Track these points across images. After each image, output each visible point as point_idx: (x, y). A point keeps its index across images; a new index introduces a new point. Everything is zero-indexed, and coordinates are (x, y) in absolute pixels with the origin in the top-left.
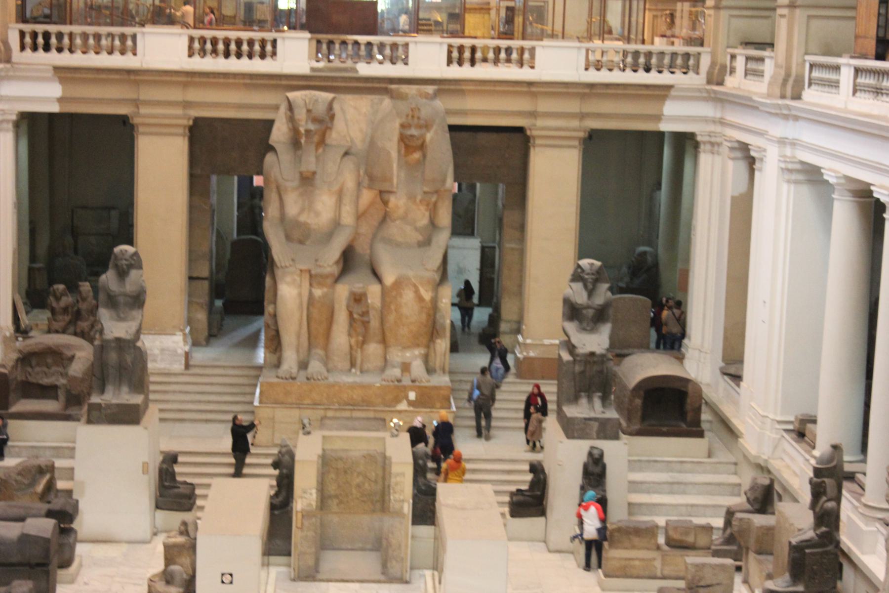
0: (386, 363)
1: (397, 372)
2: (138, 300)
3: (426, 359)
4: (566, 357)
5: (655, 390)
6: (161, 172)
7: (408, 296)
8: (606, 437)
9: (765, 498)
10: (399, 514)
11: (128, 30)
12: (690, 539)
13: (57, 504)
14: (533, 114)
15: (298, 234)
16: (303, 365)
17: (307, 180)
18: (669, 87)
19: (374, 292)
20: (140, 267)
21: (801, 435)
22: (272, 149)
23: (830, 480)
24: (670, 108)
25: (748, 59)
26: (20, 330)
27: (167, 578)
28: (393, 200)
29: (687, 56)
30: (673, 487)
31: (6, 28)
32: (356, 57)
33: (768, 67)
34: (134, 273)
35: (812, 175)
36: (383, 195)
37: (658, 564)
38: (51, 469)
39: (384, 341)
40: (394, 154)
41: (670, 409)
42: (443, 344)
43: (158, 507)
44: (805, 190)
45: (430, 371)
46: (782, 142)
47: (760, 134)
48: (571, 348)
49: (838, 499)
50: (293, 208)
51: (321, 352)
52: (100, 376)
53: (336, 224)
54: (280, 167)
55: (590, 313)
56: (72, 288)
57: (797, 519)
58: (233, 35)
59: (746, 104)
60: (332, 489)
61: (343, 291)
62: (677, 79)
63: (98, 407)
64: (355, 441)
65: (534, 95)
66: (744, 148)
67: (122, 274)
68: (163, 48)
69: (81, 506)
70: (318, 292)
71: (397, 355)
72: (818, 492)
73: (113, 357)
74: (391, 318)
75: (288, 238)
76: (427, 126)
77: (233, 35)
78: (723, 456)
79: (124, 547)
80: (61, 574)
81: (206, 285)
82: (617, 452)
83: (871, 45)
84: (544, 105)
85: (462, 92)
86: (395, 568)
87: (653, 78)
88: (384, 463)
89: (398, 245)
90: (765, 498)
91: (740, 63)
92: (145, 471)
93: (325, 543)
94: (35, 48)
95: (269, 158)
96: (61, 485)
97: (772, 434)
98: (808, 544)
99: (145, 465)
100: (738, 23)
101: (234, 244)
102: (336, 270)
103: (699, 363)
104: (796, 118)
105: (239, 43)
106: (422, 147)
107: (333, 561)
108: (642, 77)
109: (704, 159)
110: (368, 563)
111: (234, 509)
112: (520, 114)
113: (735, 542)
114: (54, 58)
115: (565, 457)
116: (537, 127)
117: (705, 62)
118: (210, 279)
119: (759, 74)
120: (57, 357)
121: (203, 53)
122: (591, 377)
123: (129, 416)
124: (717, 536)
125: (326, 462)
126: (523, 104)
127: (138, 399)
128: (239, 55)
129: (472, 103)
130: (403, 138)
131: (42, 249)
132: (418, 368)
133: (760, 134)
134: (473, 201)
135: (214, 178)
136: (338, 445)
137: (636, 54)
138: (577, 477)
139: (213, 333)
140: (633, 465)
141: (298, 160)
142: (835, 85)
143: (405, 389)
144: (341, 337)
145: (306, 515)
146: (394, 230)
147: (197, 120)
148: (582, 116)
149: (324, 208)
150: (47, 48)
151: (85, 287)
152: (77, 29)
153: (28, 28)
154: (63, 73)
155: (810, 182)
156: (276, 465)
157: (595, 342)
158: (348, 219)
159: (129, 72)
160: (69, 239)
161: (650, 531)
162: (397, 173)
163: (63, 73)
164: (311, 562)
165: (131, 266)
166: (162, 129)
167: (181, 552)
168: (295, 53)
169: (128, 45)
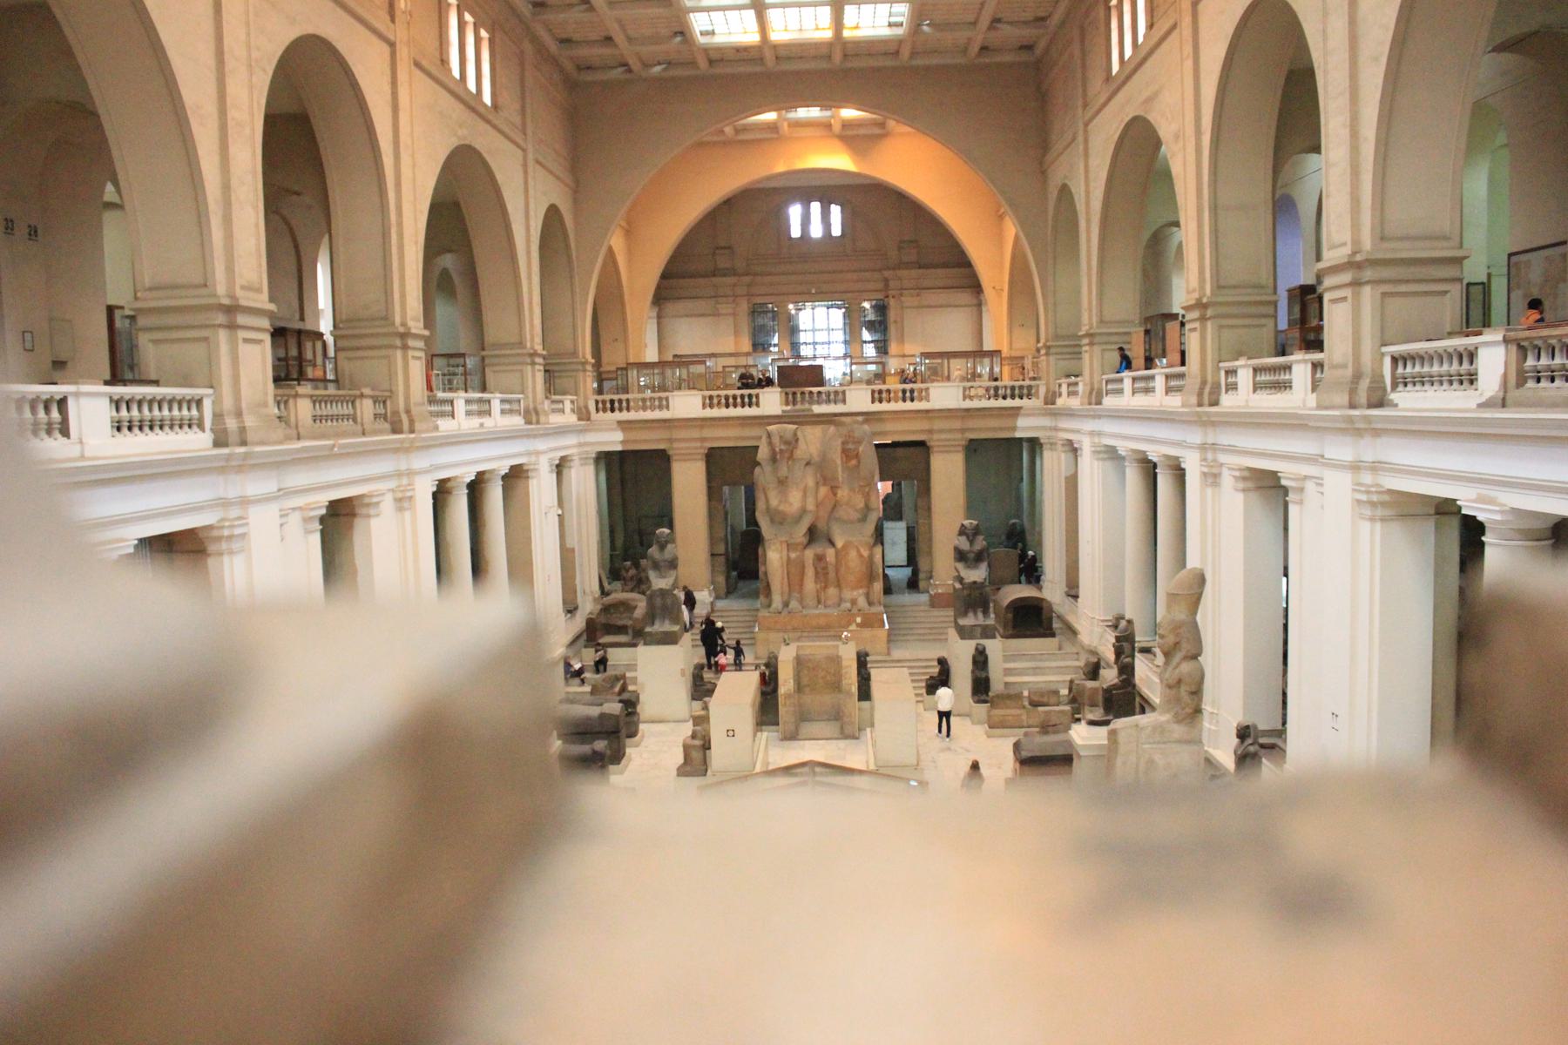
0: (841, 600)
1: (848, 605)
2: (673, 564)
3: (867, 595)
4: (958, 586)
5: (1023, 607)
6: (688, 483)
7: (853, 554)
8: (987, 637)
9: (1094, 671)
10: (849, 693)
11: (663, 395)
12: (1045, 700)
13: (625, 696)
14: (930, 432)
15: (778, 519)
16: (786, 605)
17: (782, 483)
18: (1019, 408)
19: (830, 553)
20: (673, 541)
21: (1116, 627)
22: (759, 464)
23: (1125, 644)
24: (1022, 422)
25: (1069, 385)
26: (604, 593)
27: (694, 736)
28: (840, 493)
29: (1030, 388)
30: (1036, 671)
31: (586, 398)
32: (811, 403)
33: (1080, 388)
34: (669, 546)
35: (1112, 454)
36: (834, 490)
37: (1024, 717)
38: (624, 677)
39: (839, 586)
40: (839, 462)
41: (1031, 620)
42: (878, 586)
43: (694, 699)
44: (1108, 464)
45: (870, 604)
46: (1092, 433)
47: (1078, 431)
48: (960, 579)
49: (1133, 657)
50: (774, 502)
51: (796, 595)
52: (651, 617)
53: (804, 511)
54: (764, 476)
55: (972, 556)
56: (637, 565)
57: (1110, 676)
58: (730, 393)
59: (1070, 413)
60: (805, 681)
61: (809, 554)
62: (1025, 402)
63: (650, 634)
64: (817, 648)
65: (930, 419)
66: (1070, 442)
67: (662, 547)
68: (686, 404)
69: (642, 698)
70: (793, 555)
71: (848, 594)
72: (1119, 652)
73: (658, 602)
74: (843, 570)
75: (772, 521)
76: (859, 442)
77: (730, 393)
78: (1069, 648)
79: (672, 725)
80: (628, 741)
81: (722, 559)
82: (995, 648)
83: (1142, 361)
84: (938, 425)
85: (881, 420)
86: (848, 730)
87: (1009, 403)
88: (836, 660)
89: (845, 522)
90: (1094, 671)
91: (1064, 389)
92: (683, 674)
93: (803, 717)
94: (605, 410)
95: (757, 470)
96: (631, 688)
97: (1098, 630)
98: (1114, 687)
99: (683, 673)
100: (1062, 363)
101: (745, 534)
102: (805, 541)
103: (1052, 590)
104: (1100, 417)
105: (735, 397)
106: (857, 456)
107: (808, 728)
108: (1001, 403)
109: (1047, 454)
110: (830, 728)
111: (737, 690)
112: (922, 431)
113: (1077, 701)
114: (618, 416)
115: (960, 654)
116: (934, 441)
117: (1042, 391)
118: (726, 554)
119: (1075, 393)
120: (627, 607)
121: (711, 406)
122: (973, 599)
123: (669, 639)
124: (1066, 700)
125: (799, 662)
126: (925, 425)
127: (676, 628)
128: (735, 406)
129: (889, 427)
130: (845, 451)
131: (619, 542)
132: (862, 602)
133: (1078, 431)
134: (901, 497)
135: (726, 489)
136: (807, 652)
137: (996, 389)
138: (969, 666)
139: (730, 591)
140: (1007, 659)
141: (775, 470)
142: (1120, 391)
143: (855, 616)
144: (810, 585)
145: (788, 696)
146: (842, 513)
147: (711, 449)
148: (963, 431)
149: (794, 500)
150: (613, 410)
151: (643, 562)
152: (629, 396)
153: (600, 398)
154: (624, 425)
155: (1112, 459)
156: (767, 665)
157: (978, 574)
158: (811, 506)
159: (665, 421)
160: (636, 538)
161: (1018, 697)
162: (840, 475)
163: (624, 425)
164: (792, 728)
165: (667, 542)
166: (688, 457)
167: (701, 721)
168: (771, 401)
169: (664, 404)
